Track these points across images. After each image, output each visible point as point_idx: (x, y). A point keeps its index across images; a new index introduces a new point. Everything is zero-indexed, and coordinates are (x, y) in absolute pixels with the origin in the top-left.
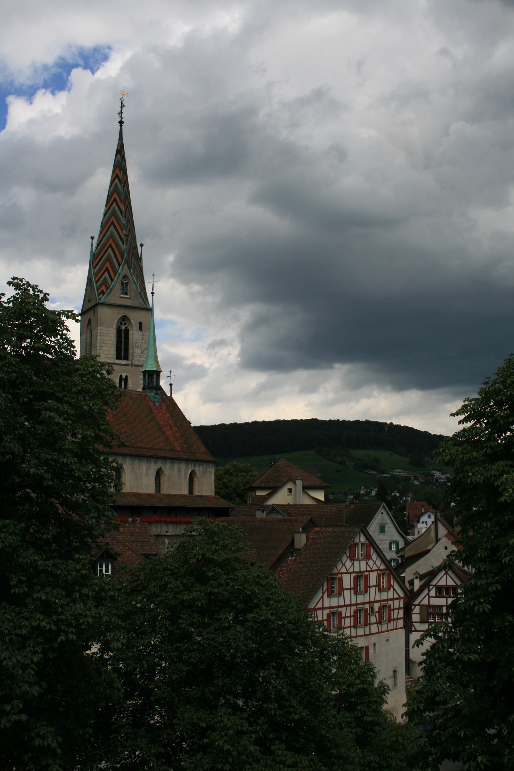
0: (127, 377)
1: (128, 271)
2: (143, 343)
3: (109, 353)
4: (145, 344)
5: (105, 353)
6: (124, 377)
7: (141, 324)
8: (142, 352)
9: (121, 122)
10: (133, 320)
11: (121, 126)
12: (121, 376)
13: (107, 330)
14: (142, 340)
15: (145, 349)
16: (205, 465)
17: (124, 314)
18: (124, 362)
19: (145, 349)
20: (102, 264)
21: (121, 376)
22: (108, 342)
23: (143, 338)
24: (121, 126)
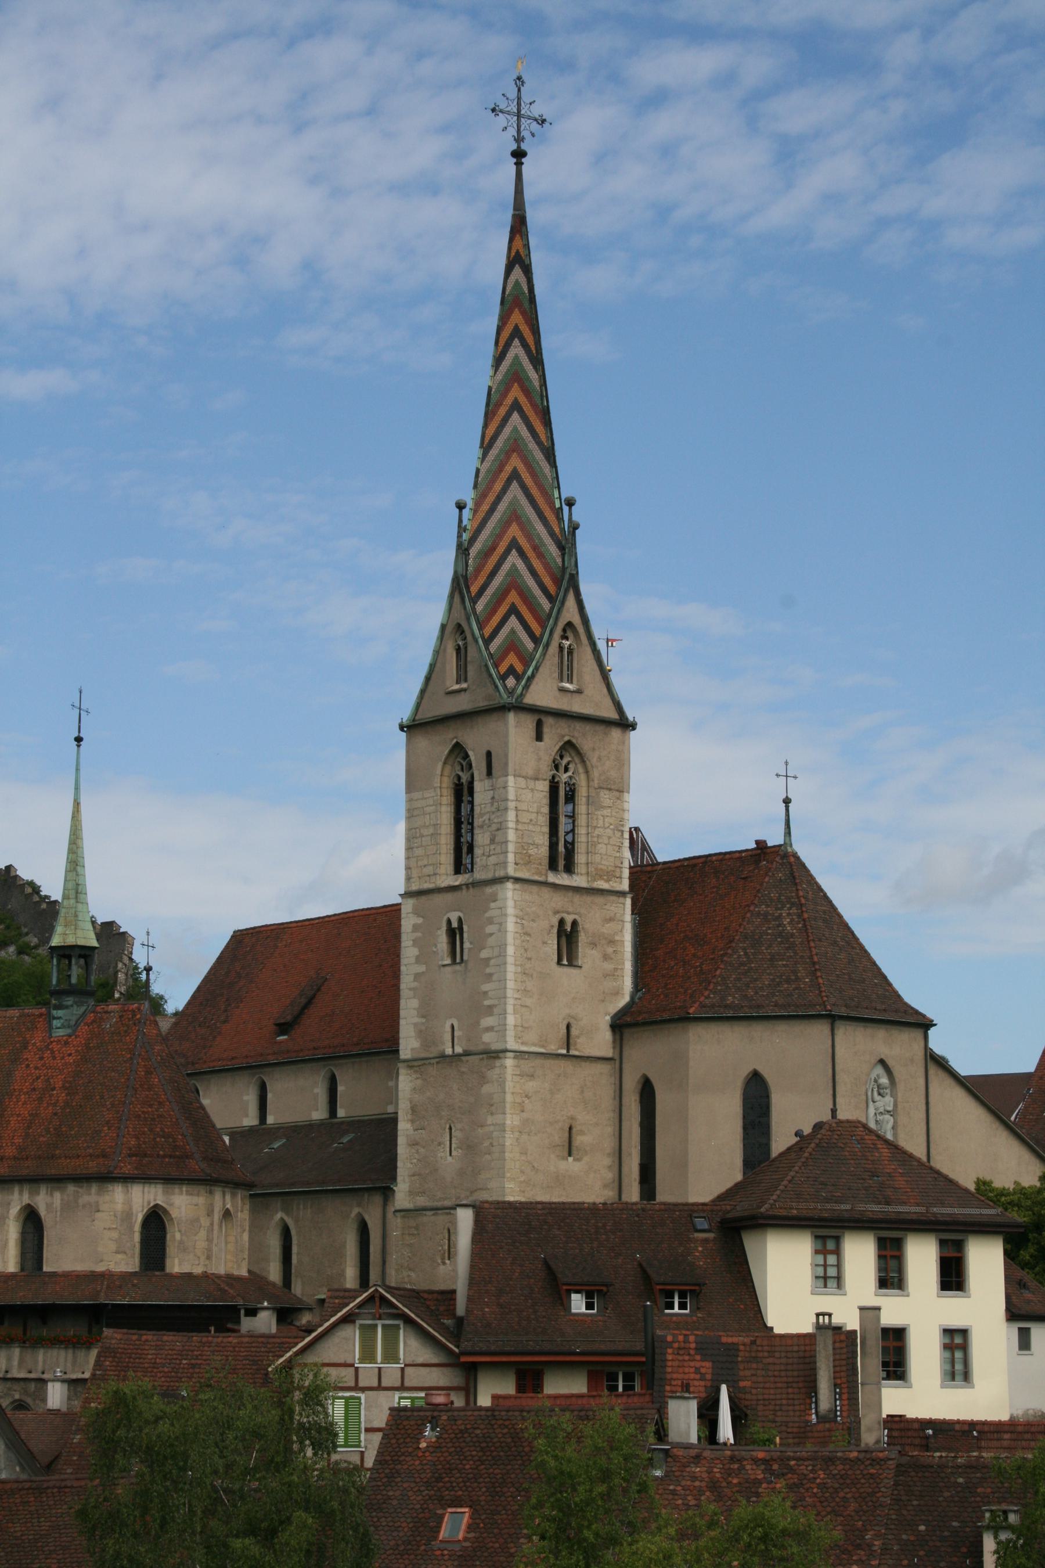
0: (460, 920)
1: (463, 611)
2: (493, 813)
3: (426, 863)
4: (499, 814)
5: (420, 863)
6: (455, 925)
7: (489, 754)
8: (492, 841)
9: (519, 155)
10: (473, 751)
11: (519, 164)
12: (449, 922)
13: (424, 798)
14: (492, 804)
15: (498, 830)
16: (71, 1188)
17: (455, 741)
18: (460, 880)
19: (498, 830)
20: (494, 594)
21: (449, 922)
22: (425, 832)
23: (493, 798)
24: (519, 164)
